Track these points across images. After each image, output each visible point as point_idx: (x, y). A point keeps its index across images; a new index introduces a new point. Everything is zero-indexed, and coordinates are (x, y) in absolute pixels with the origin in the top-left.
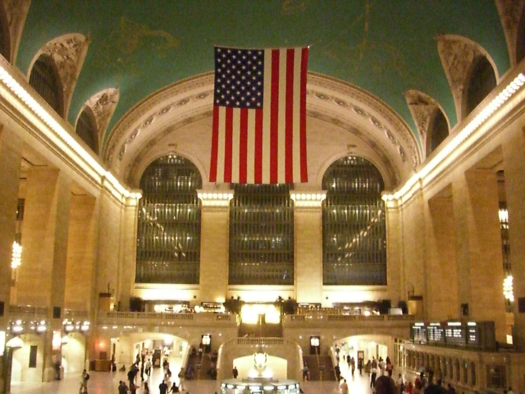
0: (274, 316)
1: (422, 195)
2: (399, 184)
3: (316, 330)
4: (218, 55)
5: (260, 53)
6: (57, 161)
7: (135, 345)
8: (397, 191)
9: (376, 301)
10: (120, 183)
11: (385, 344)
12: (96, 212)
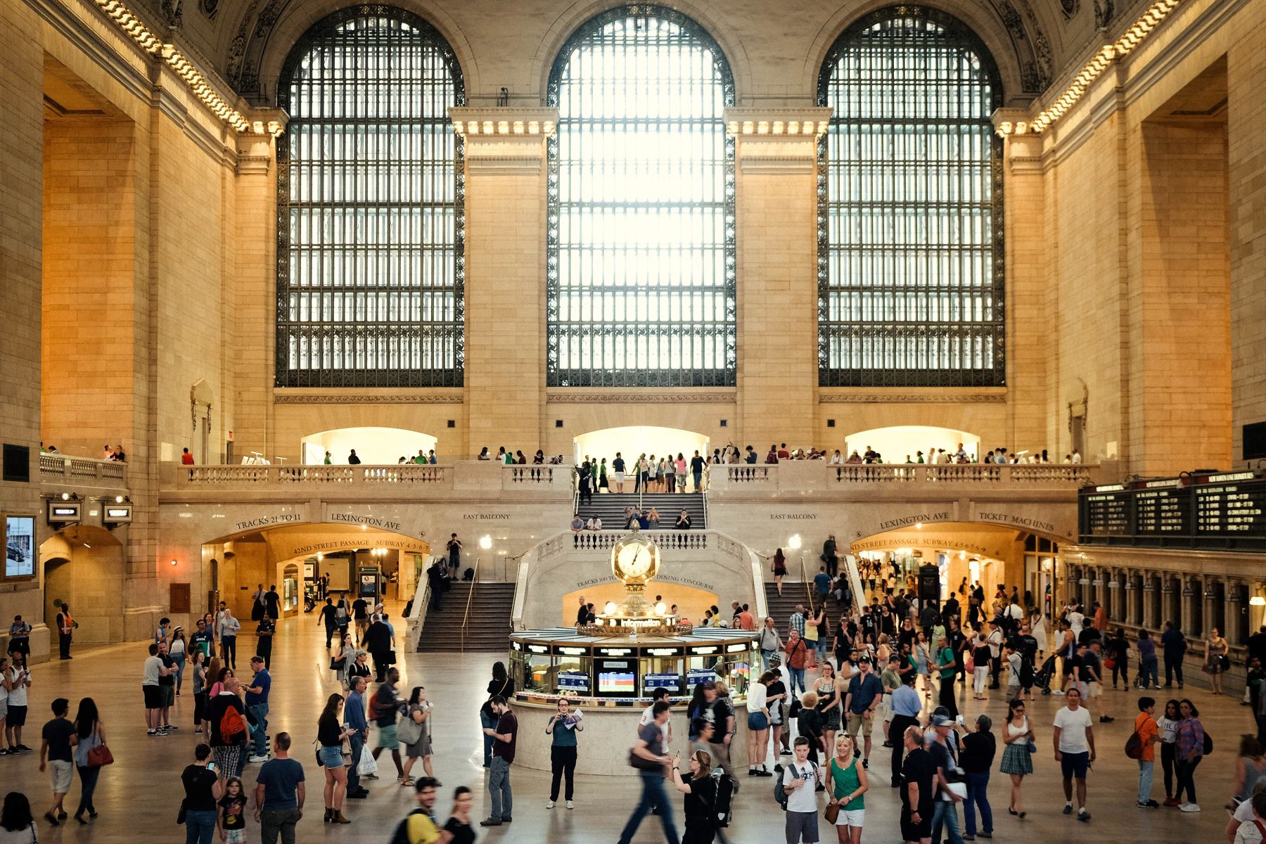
1: (1122, 109)
2: (1050, 84)
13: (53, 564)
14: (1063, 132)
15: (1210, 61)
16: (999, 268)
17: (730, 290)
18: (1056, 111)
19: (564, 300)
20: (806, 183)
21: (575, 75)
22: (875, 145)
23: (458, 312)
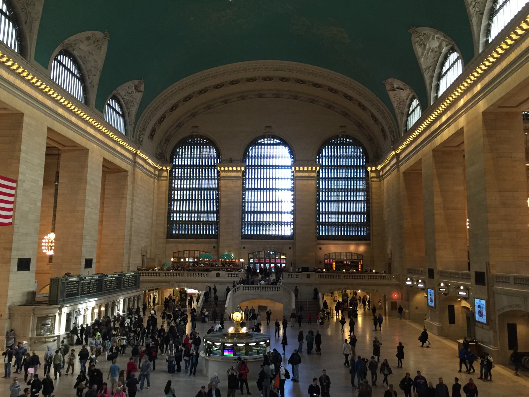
1: (398, 167)
8: (380, 164)
14: (385, 171)
15: (417, 160)
17: (291, 213)
18: (383, 165)
19: (246, 215)
21: (251, 154)
23: (217, 218)
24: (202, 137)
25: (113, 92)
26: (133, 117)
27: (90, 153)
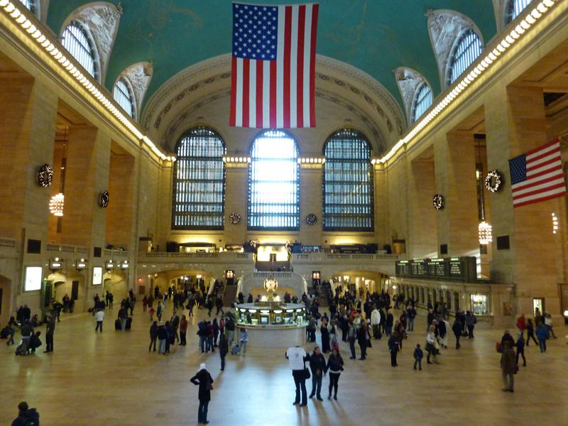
0: (282, 256)
1: (406, 157)
2: (386, 150)
3: (317, 266)
4: (235, 11)
5: (274, 9)
6: (94, 120)
7: (171, 281)
9: (366, 244)
10: (157, 146)
11: (373, 279)
12: (136, 169)
13: (106, 280)
15: (429, 146)
16: (372, 199)
19: (252, 207)
20: (320, 176)
22: (338, 165)
24: (207, 128)
25: (123, 72)
26: (140, 102)
27: (99, 132)
